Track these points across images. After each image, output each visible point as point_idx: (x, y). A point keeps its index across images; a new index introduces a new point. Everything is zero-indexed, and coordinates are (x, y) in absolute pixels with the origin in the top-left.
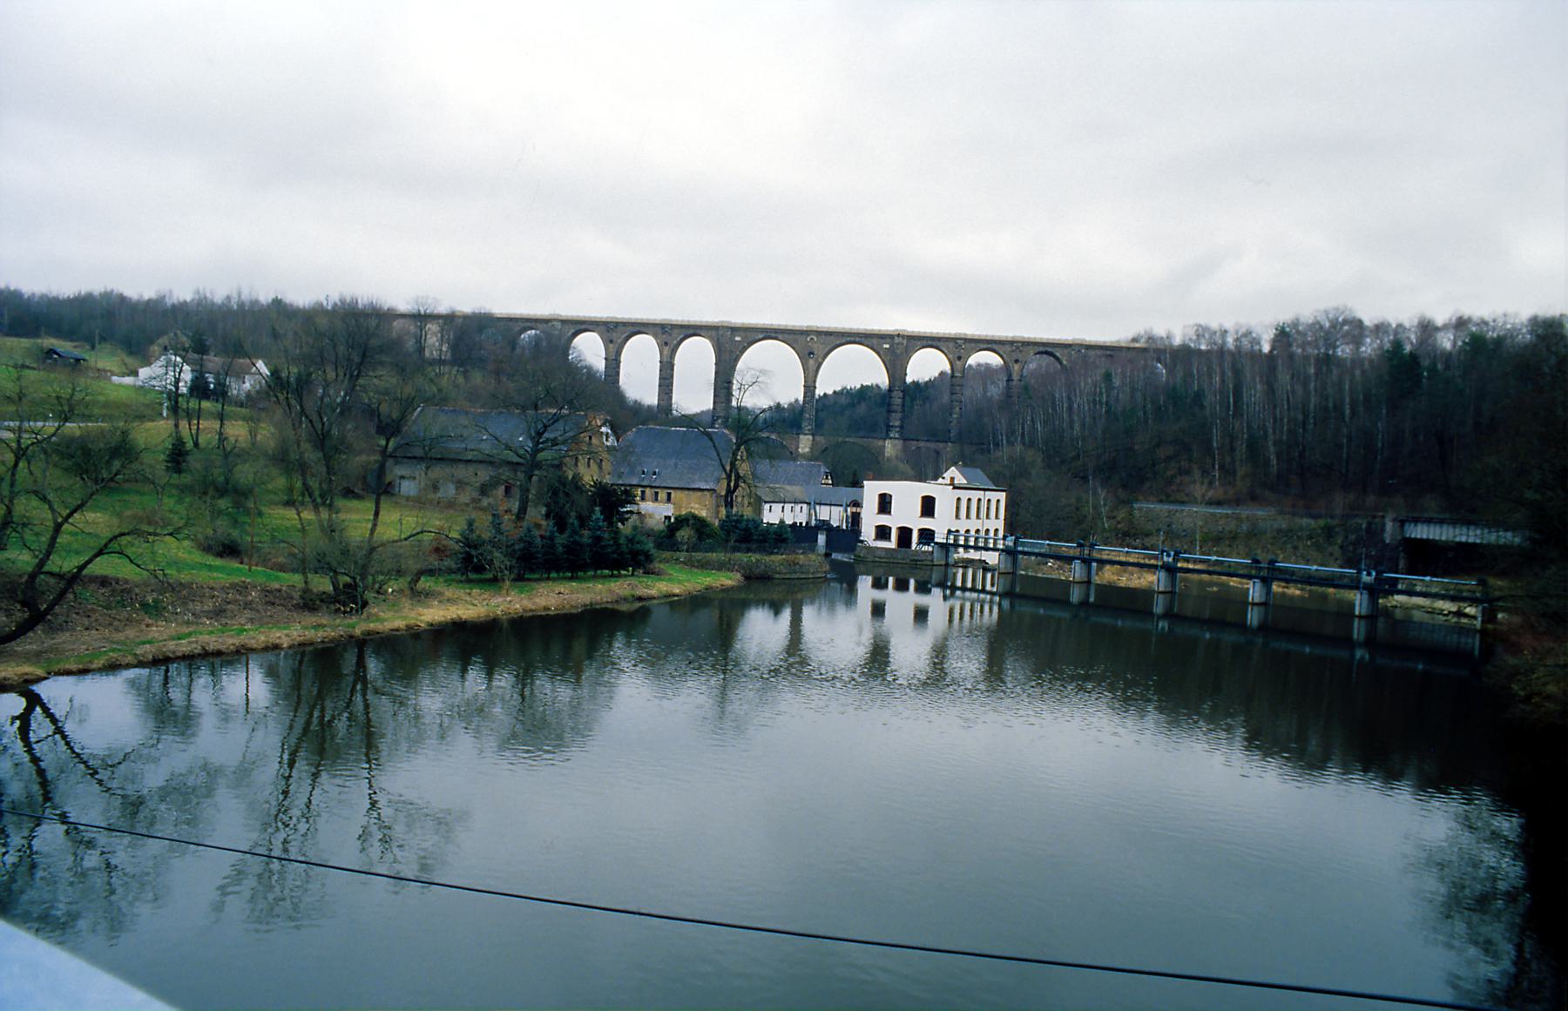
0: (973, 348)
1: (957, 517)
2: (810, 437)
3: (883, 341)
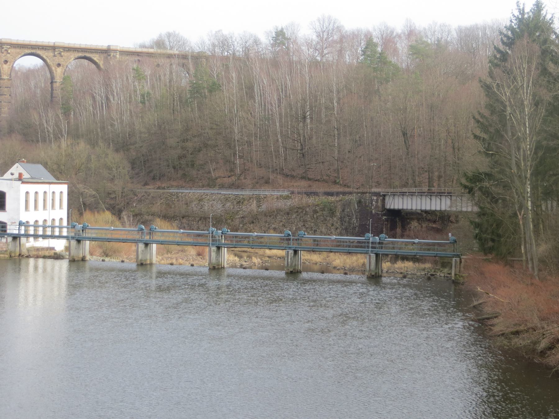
0: (19, 53)
1: (27, 208)
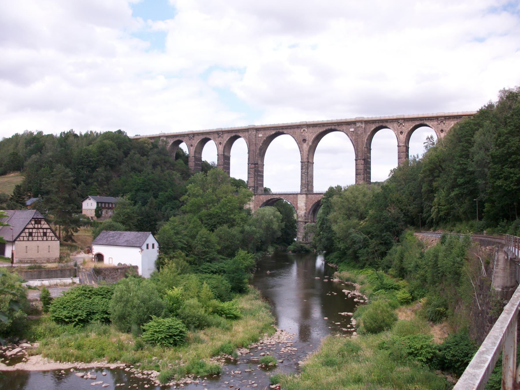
2: (304, 196)
3: (349, 127)
